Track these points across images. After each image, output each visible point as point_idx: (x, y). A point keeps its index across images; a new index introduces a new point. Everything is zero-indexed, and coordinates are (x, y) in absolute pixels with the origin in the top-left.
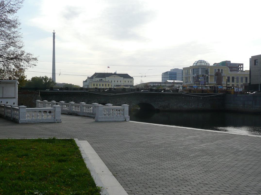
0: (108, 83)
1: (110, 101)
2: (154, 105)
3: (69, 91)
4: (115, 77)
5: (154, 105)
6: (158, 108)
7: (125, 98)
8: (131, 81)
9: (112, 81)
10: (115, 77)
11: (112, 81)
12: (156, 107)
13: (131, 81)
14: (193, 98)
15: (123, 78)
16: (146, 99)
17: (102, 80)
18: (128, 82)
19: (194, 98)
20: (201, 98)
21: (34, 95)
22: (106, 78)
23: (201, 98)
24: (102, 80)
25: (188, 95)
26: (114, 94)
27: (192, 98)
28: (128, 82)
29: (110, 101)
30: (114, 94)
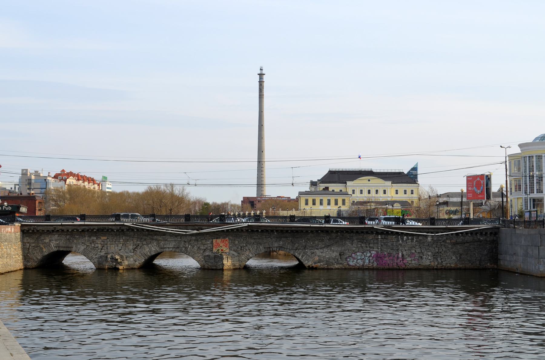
0: (344, 197)
1: (190, 247)
2: (302, 256)
3: (86, 223)
4: (369, 180)
5: (302, 256)
6: (313, 265)
8: (412, 191)
9: (353, 191)
10: (369, 180)
11: (353, 191)
12: (307, 262)
13: (412, 191)
14: (408, 239)
15: (390, 182)
16: (281, 243)
17: (327, 188)
18: (405, 192)
19: (410, 238)
20: (429, 239)
22: (346, 183)
23: (429, 239)
24: (327, 188)
25: (392, 232)
26: (195, 232)
27: (402, 239)
28: (405, 192)
29: (190, 247)
30: (195, 232)
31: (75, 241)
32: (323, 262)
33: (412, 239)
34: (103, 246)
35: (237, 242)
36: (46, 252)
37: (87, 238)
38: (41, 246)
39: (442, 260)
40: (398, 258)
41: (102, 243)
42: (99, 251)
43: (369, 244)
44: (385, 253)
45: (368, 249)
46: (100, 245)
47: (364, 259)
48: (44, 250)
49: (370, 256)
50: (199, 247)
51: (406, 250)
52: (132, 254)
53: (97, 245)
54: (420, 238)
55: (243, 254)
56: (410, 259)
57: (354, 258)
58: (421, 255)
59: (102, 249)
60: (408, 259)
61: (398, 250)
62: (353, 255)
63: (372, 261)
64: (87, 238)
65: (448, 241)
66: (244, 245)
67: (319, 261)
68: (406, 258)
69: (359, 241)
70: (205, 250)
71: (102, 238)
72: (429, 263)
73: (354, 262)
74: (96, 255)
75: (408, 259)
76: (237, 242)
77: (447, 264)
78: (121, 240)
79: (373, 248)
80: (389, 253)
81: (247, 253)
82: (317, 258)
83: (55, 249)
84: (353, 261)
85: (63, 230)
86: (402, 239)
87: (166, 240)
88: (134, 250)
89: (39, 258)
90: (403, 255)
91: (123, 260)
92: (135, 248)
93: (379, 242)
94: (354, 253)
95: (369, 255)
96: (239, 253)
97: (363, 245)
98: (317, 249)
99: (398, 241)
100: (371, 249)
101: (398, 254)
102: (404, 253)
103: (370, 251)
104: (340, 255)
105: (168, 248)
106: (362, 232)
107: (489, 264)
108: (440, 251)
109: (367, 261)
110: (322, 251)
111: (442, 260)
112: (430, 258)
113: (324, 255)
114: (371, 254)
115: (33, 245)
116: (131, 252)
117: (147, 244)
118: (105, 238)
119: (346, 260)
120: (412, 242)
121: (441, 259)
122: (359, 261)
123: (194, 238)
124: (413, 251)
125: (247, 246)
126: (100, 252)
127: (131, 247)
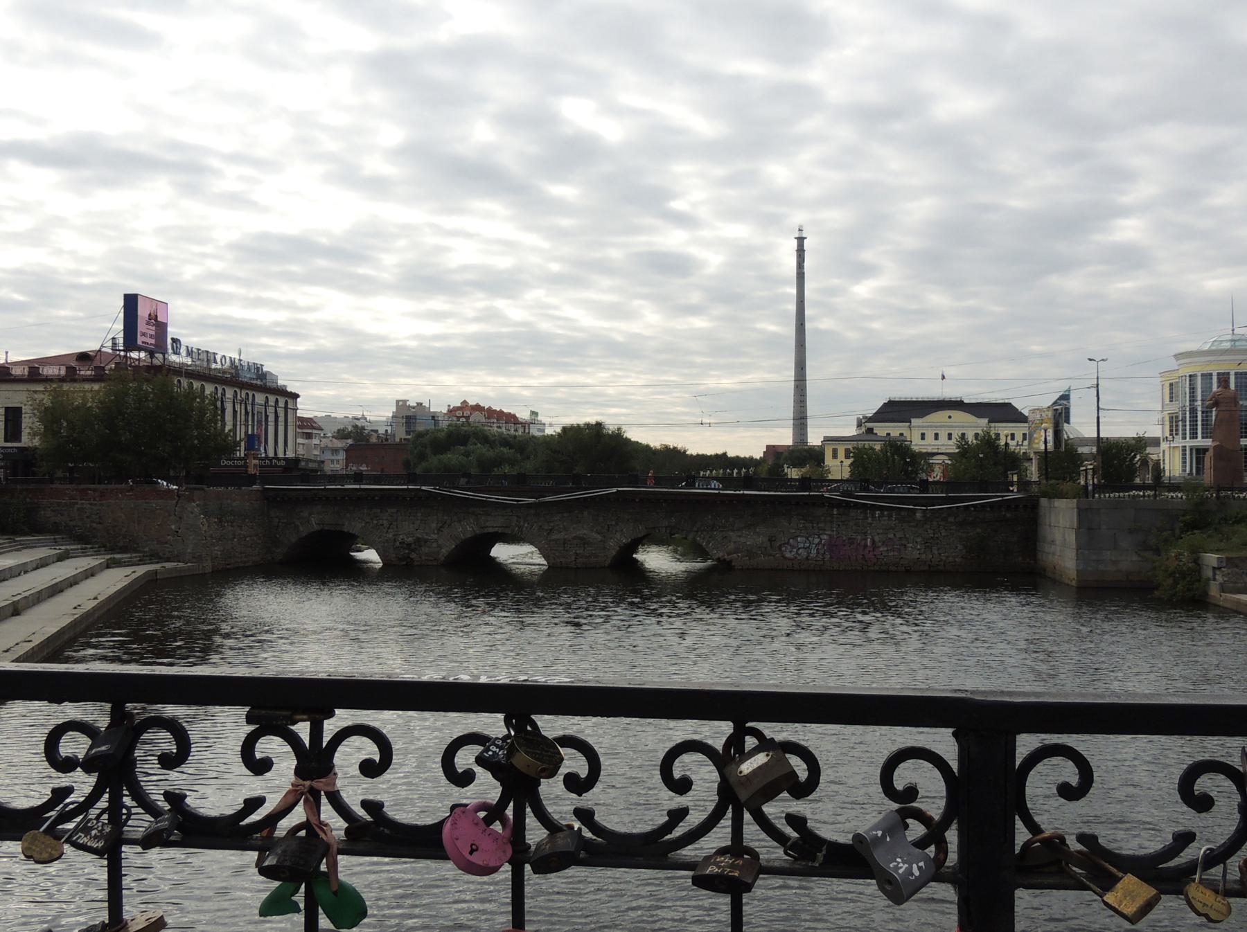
2: (708, 542)
3: (363, 487)
7: (586, 513)
14: (882, 515)
19: (886, 513)
20: (918, 515)
21: (174, 502)
27: (873, 516)
31: (348, 515)
32: (742, 552)
33: (890, 517)
34: (391, 524)
35: (601, 519)
36: (304, 530)
37: (365, 511)
38: (298, 523)
39: (940, 551)
40: (866, 546)
41: (389, 518)
42: (385, 530)
43: (818, 523)
44: (844, 538)
45: (817, 531)
46: (385, 522)
47: (809, 547)
48: (301, 529)
49: (818, 544)
50: (541, 526)
51: (878, 534)
52: (435, 536)
53: (381, 522)
54: (903, 513)
55: (611, 538)
56: (885, 549)
57: (793, 547)
58: (904, 542)
59: (389, 528)
60: (881, 549)
61: (865, 533)
62: (791, 540)
63: (822, 552)
64: (365, 511)
65: (951, 519)
66: (614, 523)
67: (737, 551)
68: (879, 547)
69: (801, 517)
70: (551, 530)
71: (389, 510)
72: (918, 556)
73: (793, 553)
74: (380, 537)
75: (881, 549)
76: (601, 519)
77: (948, 557)
78: (419, 515)
79: (825, 530)
80: (849, 539)
81: (618, 535)
82: (732, 546)
83: (316, 528)
84: (791, 552)
85: (328, 498)
86: (873, 516)
87: (489, 515)
88: (439, 530)
89: (293, 540)
90: (873, 542)
91: (420, 546)
92: (441, 527)
93: (835, 519)
94: (793, 539)
95: (817, 541)
96: (604, 537)
97: (807, 525)
98: (733, 531)
99: (867, 518)
100: (821, 532)
101: (866, 539)
102: (877, 539)
103: (819, 535)
104: (770, 541)
105: (493, 527)
106: (807, 504)
107: (1020, 559)
108: (936, 536)
109: (814, 552)
110: (739, 533)
111: (940, 551)
112: (919, 547)
113: (743, 540)
114: (821, 540)
115: (285, 521)
116: (434, 533)
117: (459, 521)
118: (395, 510)
119: (780, 549)
120: (888, 520)
121: (938, 549)
122: (800, 551)
123: (532, 511)
124: (891, 536)
125: (617, 524)
126: (387, 532)
127: (434, 525)
